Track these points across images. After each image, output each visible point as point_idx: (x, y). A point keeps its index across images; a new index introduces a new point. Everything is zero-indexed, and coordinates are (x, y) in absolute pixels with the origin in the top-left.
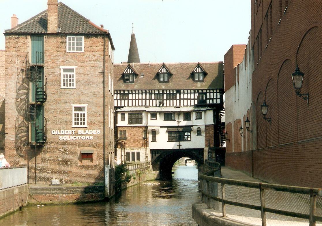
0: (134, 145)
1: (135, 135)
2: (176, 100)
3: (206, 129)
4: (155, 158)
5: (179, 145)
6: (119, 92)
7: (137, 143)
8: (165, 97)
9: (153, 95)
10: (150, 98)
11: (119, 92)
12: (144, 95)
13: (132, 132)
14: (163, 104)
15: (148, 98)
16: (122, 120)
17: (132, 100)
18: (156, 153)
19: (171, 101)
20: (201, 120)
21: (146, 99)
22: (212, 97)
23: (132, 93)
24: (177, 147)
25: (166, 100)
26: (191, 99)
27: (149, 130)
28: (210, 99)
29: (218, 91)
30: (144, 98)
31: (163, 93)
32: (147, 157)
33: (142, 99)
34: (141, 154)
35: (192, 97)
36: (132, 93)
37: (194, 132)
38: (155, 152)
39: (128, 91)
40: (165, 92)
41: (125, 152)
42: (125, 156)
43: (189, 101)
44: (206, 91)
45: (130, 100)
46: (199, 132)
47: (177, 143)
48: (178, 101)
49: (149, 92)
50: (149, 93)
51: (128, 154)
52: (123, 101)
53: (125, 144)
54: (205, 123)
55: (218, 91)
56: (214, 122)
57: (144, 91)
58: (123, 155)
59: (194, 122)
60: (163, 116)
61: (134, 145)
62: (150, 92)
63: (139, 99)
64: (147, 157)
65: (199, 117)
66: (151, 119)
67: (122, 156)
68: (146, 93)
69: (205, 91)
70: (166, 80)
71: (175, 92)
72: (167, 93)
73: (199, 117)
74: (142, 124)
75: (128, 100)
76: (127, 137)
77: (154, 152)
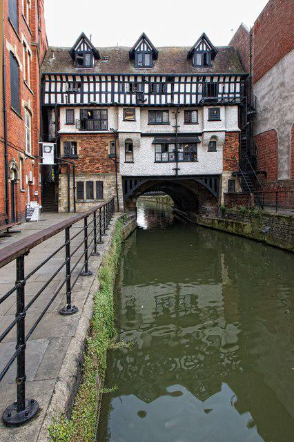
0: (91, 168)
1: (93, 150)
2: (166, 94)
3: (226, 140)
4: (130, 192)
5: (177, 170)
6: (64, 80)
7: (97, 165)
8: (146, 90)
9: (127, 86)
10: (121, 90)
11: (64, 80)
12: (110, 85)
13: (88, 146)
14: (143, 102)
15: (116, 90)
16: (67, 124)
17: (89, 93)
18: (133, 183)
19: (158, 97)
20: (218, 122)
21: (113, 93)
22: (227, 91)
23: (89, 82)
24: (173, 173)
25: (149, 94)
26: (191, 94)
27: (120, 140)
28: (224, 93)
29: (238, 80)
30: (109, 89)
31: (144, 82)
32: (117, 189)
33: (106, 93)
34: (105, 185)
35: (194, 91)
36: (89, 82)
37: (204, 145)
38: (131, 182)
39: (82, 77)
40: (147, 79)
41: (74, 182)
42: (74, 189)
43: (188, 96)
44: (219, 80)
45: (86, 93)
46: (212, 146)
47: (173, 165)
48: (169, 97)
49: (119, 79)
50: (119, 82)
51: (80, 184)
52: (72, 96)
53: (74, 167)
54: (226, 127)
55: (238, 80)
56: (240, 127)
57: (109, 79)
58: (71, 187)
59: (204, 125)
60: (147, 115)
61: (91, 168)
62: (121, 80)
63: (101, 93)
64: (117, 189)
65: (214, 117)
66: (124, 120)
67: (69, 189)
68: (113, 81)
69: (215, 80)
70: (147, 64)
71: (164, 81)
72: (149, 83)
73: (214, 117)
74: (107, 130)
75: (82, 93)
76: (78, 153)
77: (128, 183)
